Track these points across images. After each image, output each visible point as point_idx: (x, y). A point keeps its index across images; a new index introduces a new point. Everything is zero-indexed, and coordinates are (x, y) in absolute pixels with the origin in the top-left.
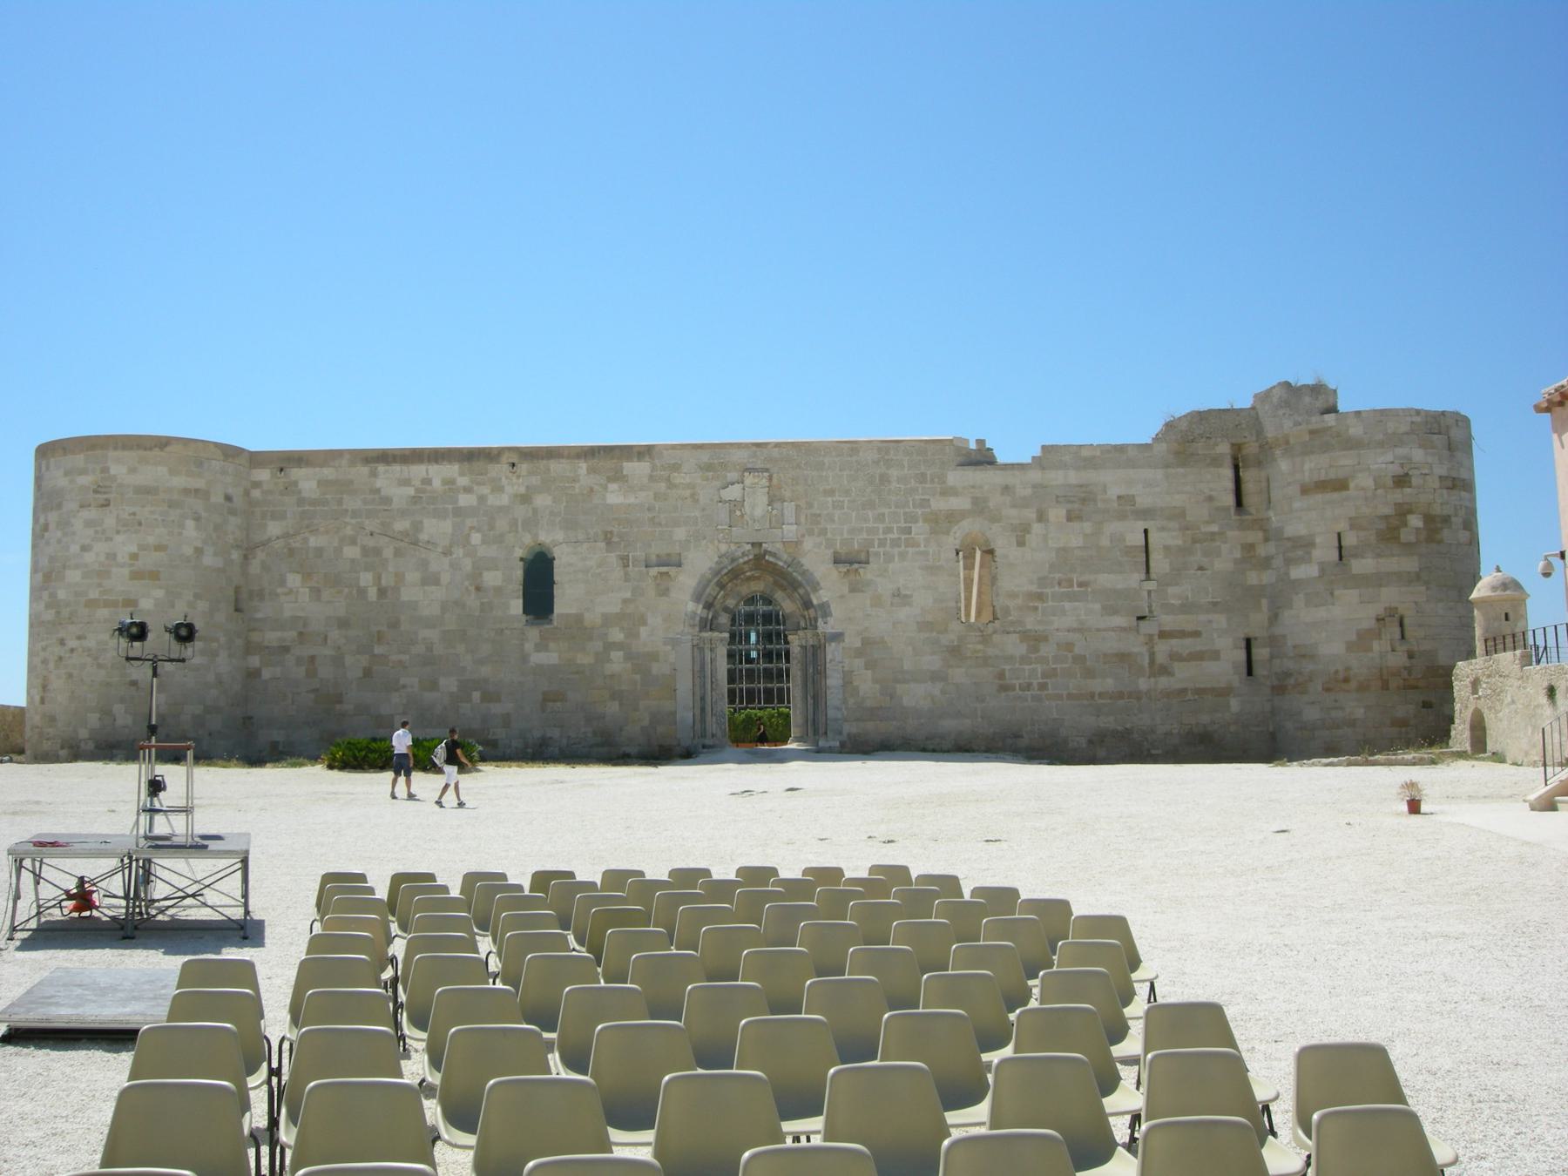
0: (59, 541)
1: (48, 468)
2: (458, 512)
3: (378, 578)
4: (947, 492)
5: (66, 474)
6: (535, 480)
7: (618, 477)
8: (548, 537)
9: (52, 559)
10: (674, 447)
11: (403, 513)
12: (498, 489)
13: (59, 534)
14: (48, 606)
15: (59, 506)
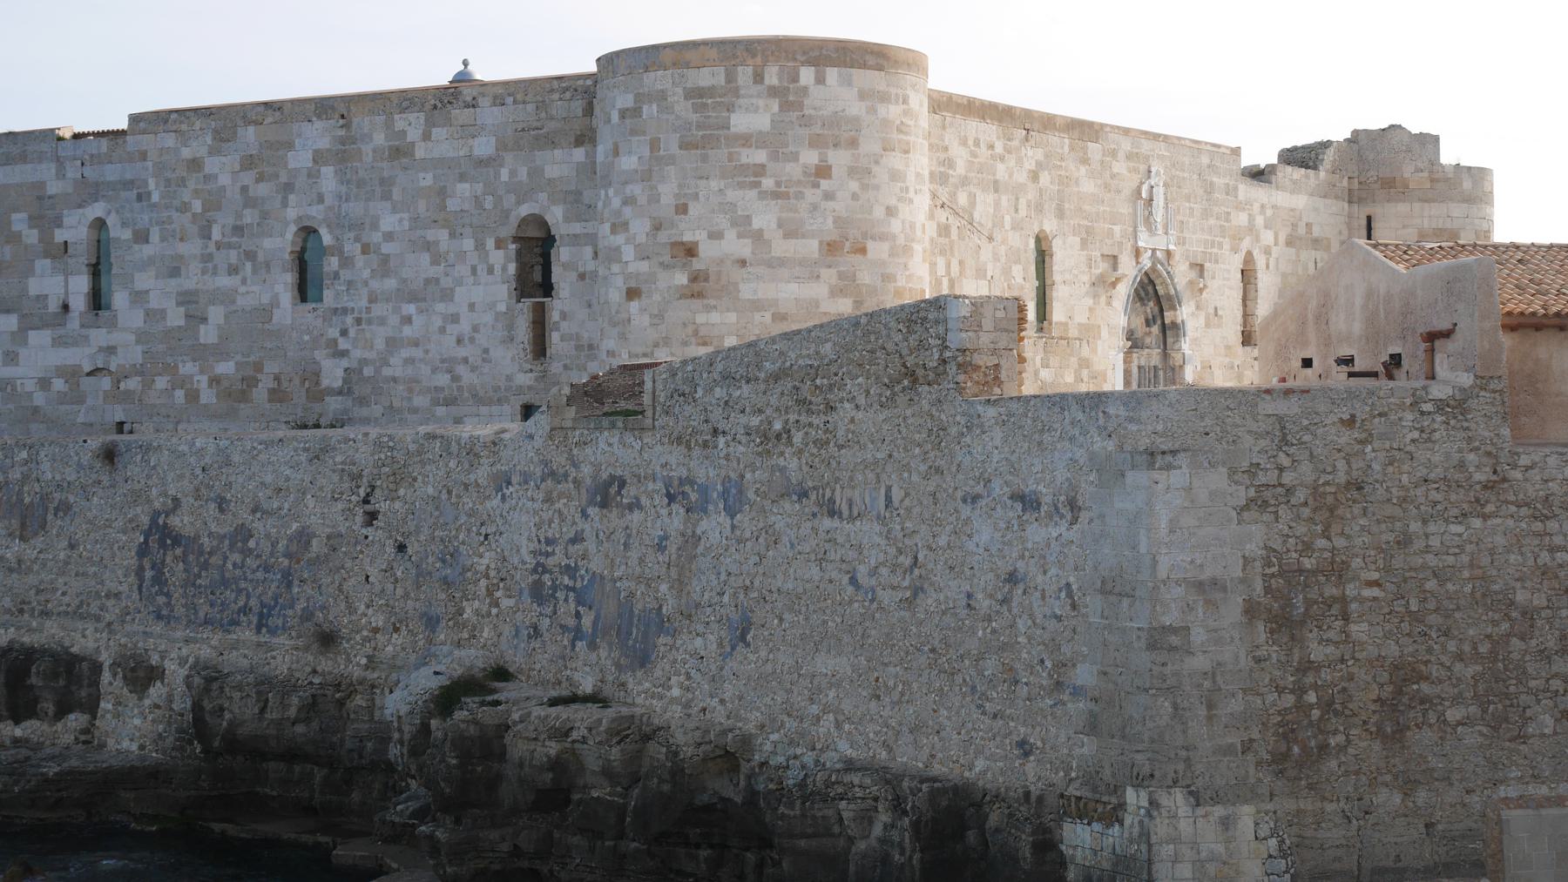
0: (855, 197)
1: (820, 80)
2: (996, 187)
3: (948, 266)
4: (1240, 207)
5: (863, 95)
6: (1039, 154)
7: (1085, 161)
8: (1050, 226)
9: (837, 220)
10: (1112, 127)
11: (965, 181)
12: (1020, 161)
13: (854, 186)
14: (836, 292)
15: (853, 143)
